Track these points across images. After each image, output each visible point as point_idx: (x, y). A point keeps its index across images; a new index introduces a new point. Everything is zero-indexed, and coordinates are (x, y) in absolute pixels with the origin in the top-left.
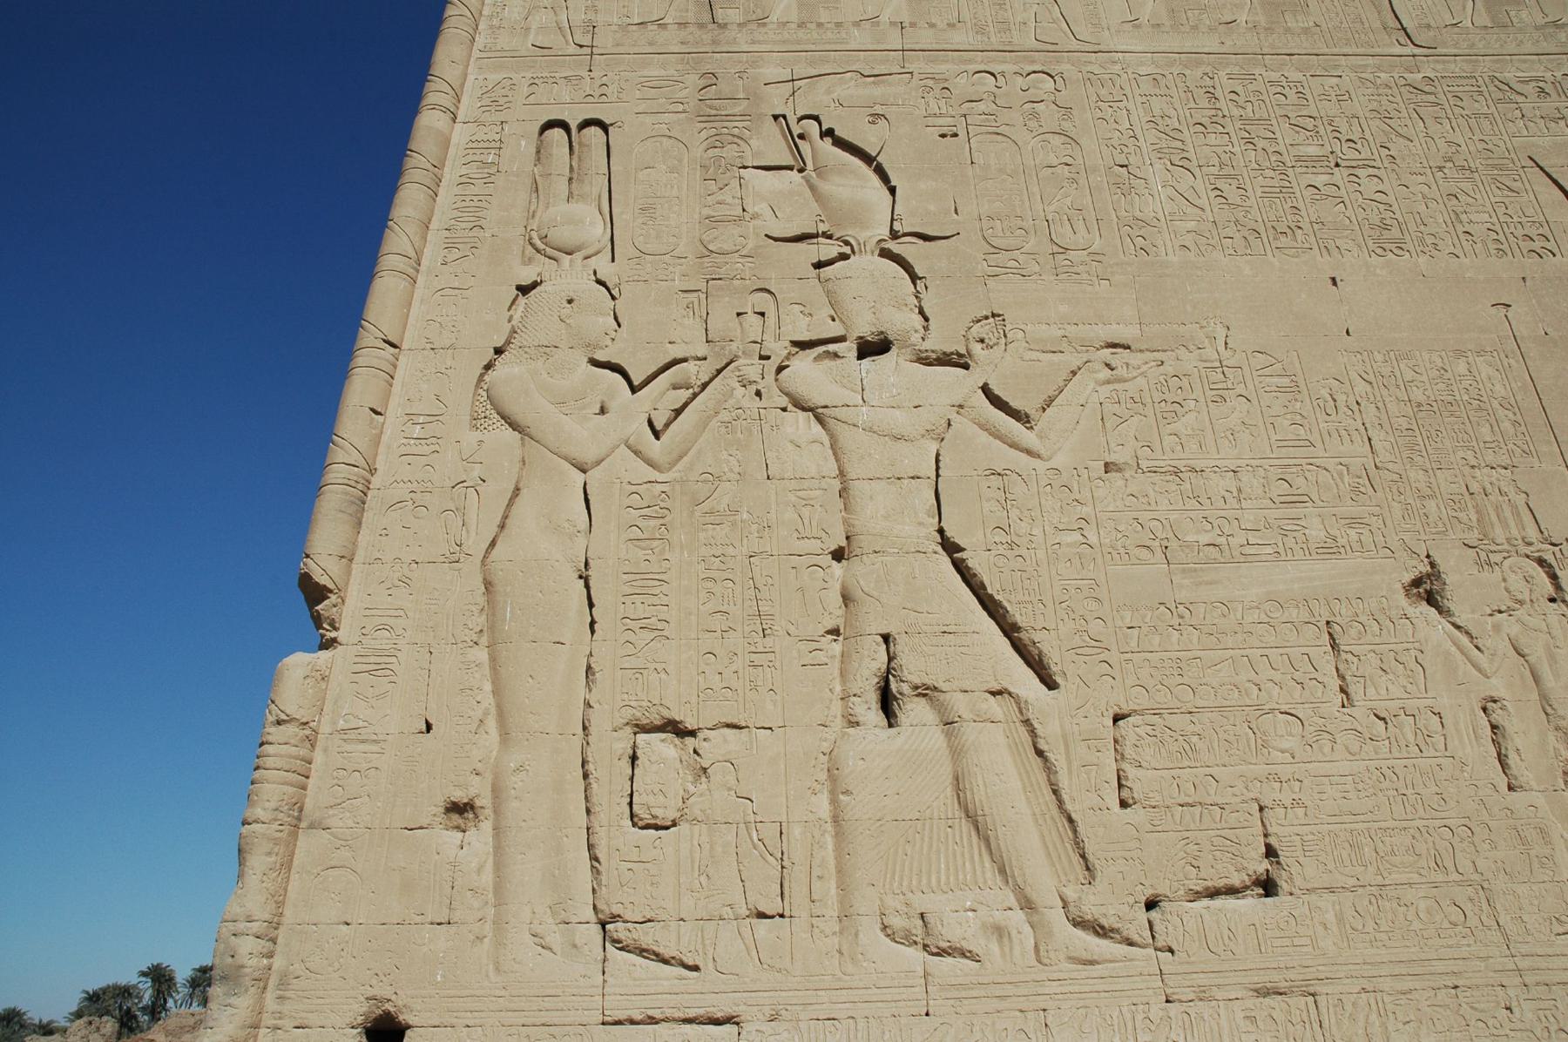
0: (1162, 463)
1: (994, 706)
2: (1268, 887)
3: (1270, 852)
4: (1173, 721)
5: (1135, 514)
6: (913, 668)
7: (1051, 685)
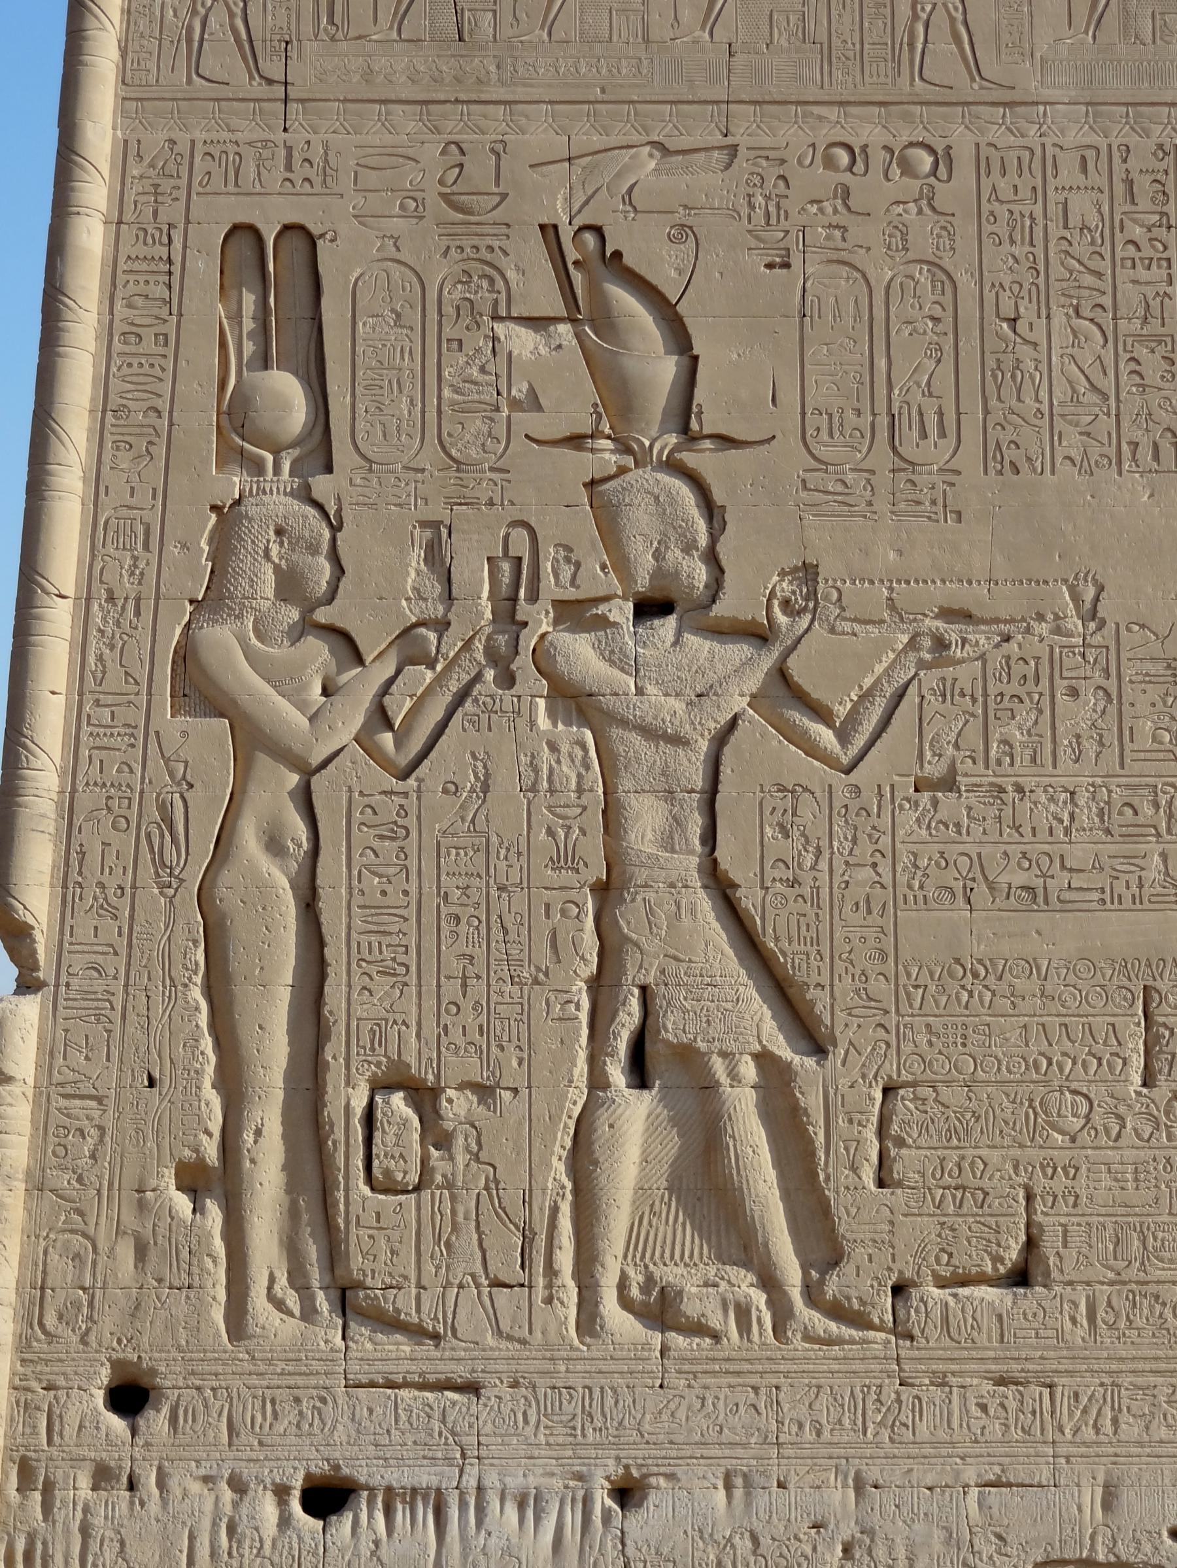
0: (985, 780)
2: (1020, 1277)
4: (945, 1092)
5: (941, 847)
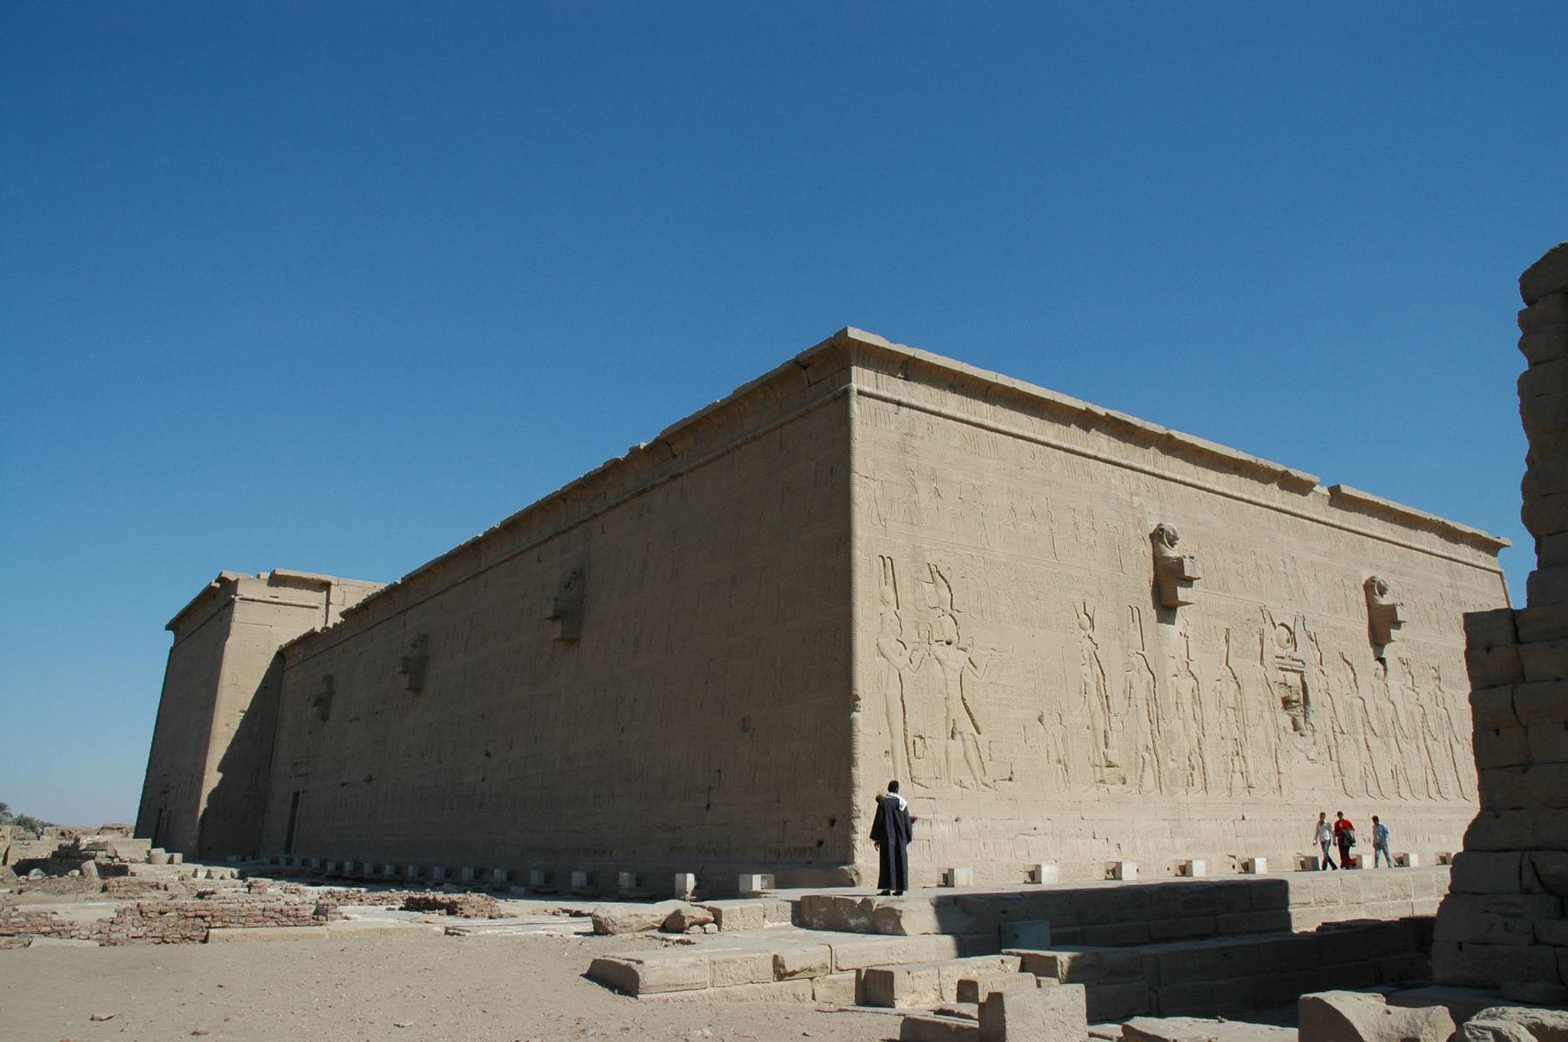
1: (970, 737)
2: (1010, 779)
3: (1012, 773)
6: (959, 727)
7: (979, 733)
